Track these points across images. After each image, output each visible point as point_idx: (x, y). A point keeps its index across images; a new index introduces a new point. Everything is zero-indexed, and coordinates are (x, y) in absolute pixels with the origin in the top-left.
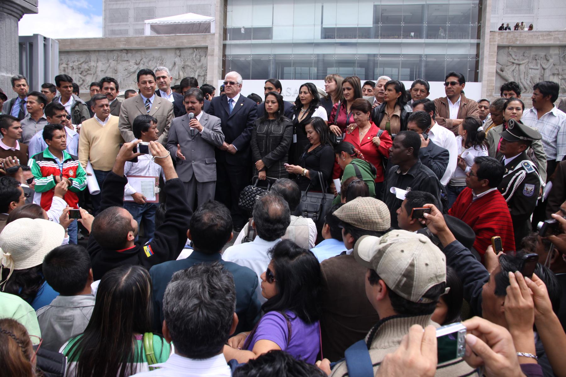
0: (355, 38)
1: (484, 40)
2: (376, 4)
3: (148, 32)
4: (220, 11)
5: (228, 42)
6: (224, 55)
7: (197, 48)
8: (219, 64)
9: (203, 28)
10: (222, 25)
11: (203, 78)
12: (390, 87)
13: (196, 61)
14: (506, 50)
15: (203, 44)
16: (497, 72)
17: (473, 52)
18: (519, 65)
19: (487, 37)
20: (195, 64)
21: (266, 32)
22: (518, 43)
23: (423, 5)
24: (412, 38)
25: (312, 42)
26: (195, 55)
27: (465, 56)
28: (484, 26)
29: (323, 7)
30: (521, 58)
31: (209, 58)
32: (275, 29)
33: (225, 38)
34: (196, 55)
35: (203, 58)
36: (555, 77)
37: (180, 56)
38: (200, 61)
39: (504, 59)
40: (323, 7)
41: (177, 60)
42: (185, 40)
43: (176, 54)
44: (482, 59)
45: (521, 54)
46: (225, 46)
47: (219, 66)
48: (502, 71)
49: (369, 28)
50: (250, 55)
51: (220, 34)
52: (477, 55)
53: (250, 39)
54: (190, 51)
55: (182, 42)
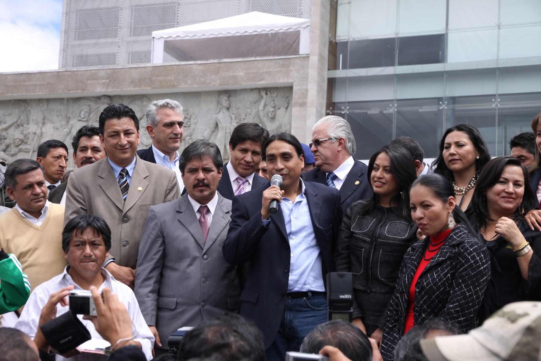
3: (159, 57)
7: (267, 90)
9: (284, 44)
10: (327, 35)
13: (265, 120)
15: (281, 80)
31: (295, 110)
33: (333, 65)
34: (265, 105)
35: (281, 112)
37: (228, 109)
38: (273, 119)
42: (242, 72)
43: (219, 103)
46: (332, 83)
51: (321, 56)
53: (393, 65)
54: (254, 96)
55: (235, 77)
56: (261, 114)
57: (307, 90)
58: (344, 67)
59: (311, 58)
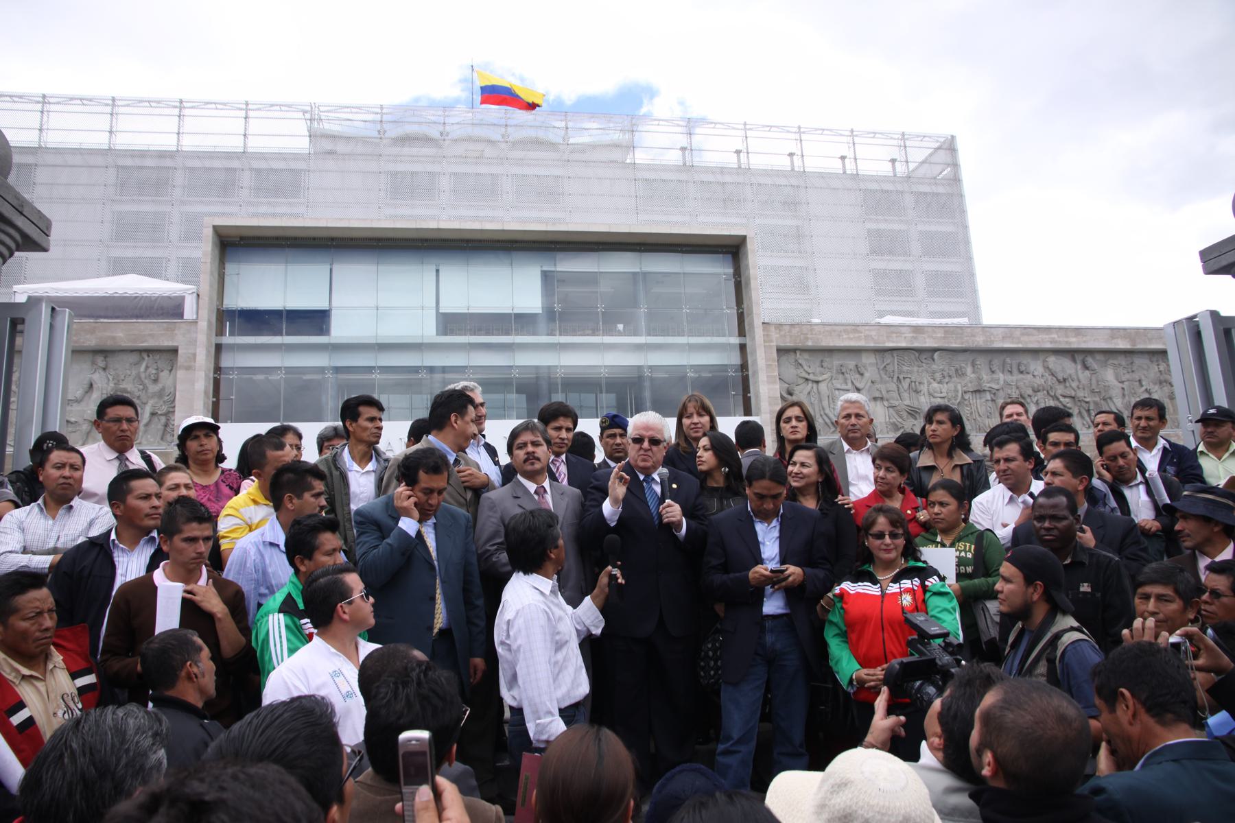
0: (507, 333)
1: (753, 339)
2: (545, 269)
5: (227, 339)
6: (218, 369)
7: (149, 351)
8: (206, 387)
9: (171, 309)
10: (215, 303)
11: (163, 419)
12: (940, 416)
14: (792, 357)
15: (167, 343)
16: (782, 397)
17: (735, 359)
18: (817, 382)
19: (759, 332)
20: (145, 388)
21: (317, 320)
22: (810, 343)
23: (635, 274)
24: (620, 334)
25: (419, 341)
26: (145, 367)
27: (723, 368)
28: (751, 313)
29: (437, 271)
30: (819, 369)
31: (180, 374)
32: (333, 312)
33: (220, 332)
34: (147, 367)
35: (164, 375)
36: (878, 403)
37: (104, 369)
38: (156, 381)
39: (791, 372)
40: (437, 271)
41: (98, 378)
42: (120, 333)
43: (93, 363)
44: (756, 372)
45: (818, 363)
46: (219, 348)
47: (206, 393)
48: (791, 394)
49: (536, 315)
50: (280, 368)
52: (744, 366)
54: (133, 358)
55: (114, 338)
56: (143, 376)
57: (194, 355)
58: (232, 334)
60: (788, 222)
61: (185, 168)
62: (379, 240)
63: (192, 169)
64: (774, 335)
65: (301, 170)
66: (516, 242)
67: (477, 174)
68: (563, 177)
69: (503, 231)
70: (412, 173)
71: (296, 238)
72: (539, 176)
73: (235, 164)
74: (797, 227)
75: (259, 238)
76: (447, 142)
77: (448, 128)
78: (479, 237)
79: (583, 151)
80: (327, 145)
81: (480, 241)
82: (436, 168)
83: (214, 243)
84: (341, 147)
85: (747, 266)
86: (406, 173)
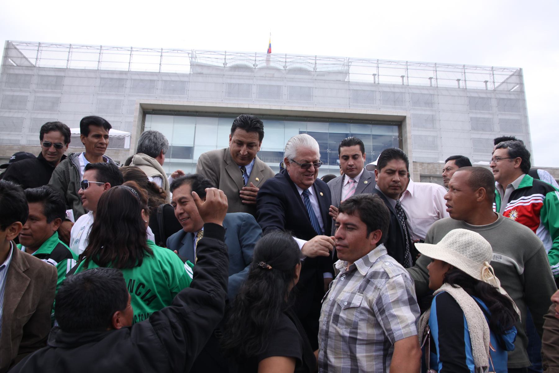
4: (138, 127)
32: (196, 149)
53: (169, 158)
59: (131, 150)
60: (429, 113)
61: (132, 79)
62: (219, 113)
63: (135, 80)
64: (419, 168)
65: (185, 82)
66: (287, 116)
67: (270, 86)
68: (313, 88)
69: (281, 110)
70: (239, 84)
71: (179, 111)
72: (301, 87)
73: (155, 78)
74: (433, 115)
75: (161, 110)
76: (256, 70)
77: (257, 63)
78: (268, 113)
79: (323, 75)
80: (199, 70)
81: (269, 115)
82: (251, 82)
83: (140, 112)
84: (205, 71)
85: (406, 132)
86: (236, 84)
